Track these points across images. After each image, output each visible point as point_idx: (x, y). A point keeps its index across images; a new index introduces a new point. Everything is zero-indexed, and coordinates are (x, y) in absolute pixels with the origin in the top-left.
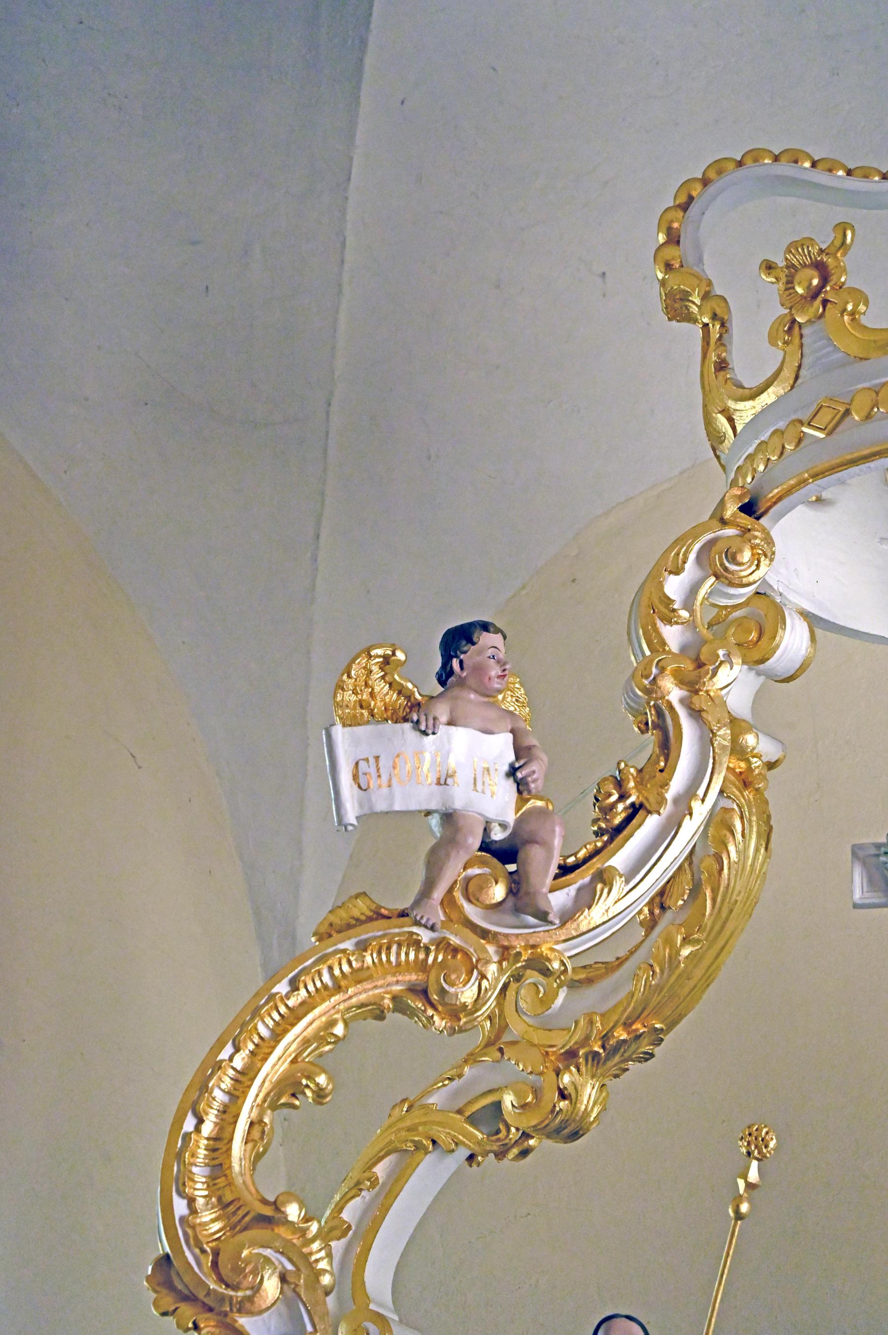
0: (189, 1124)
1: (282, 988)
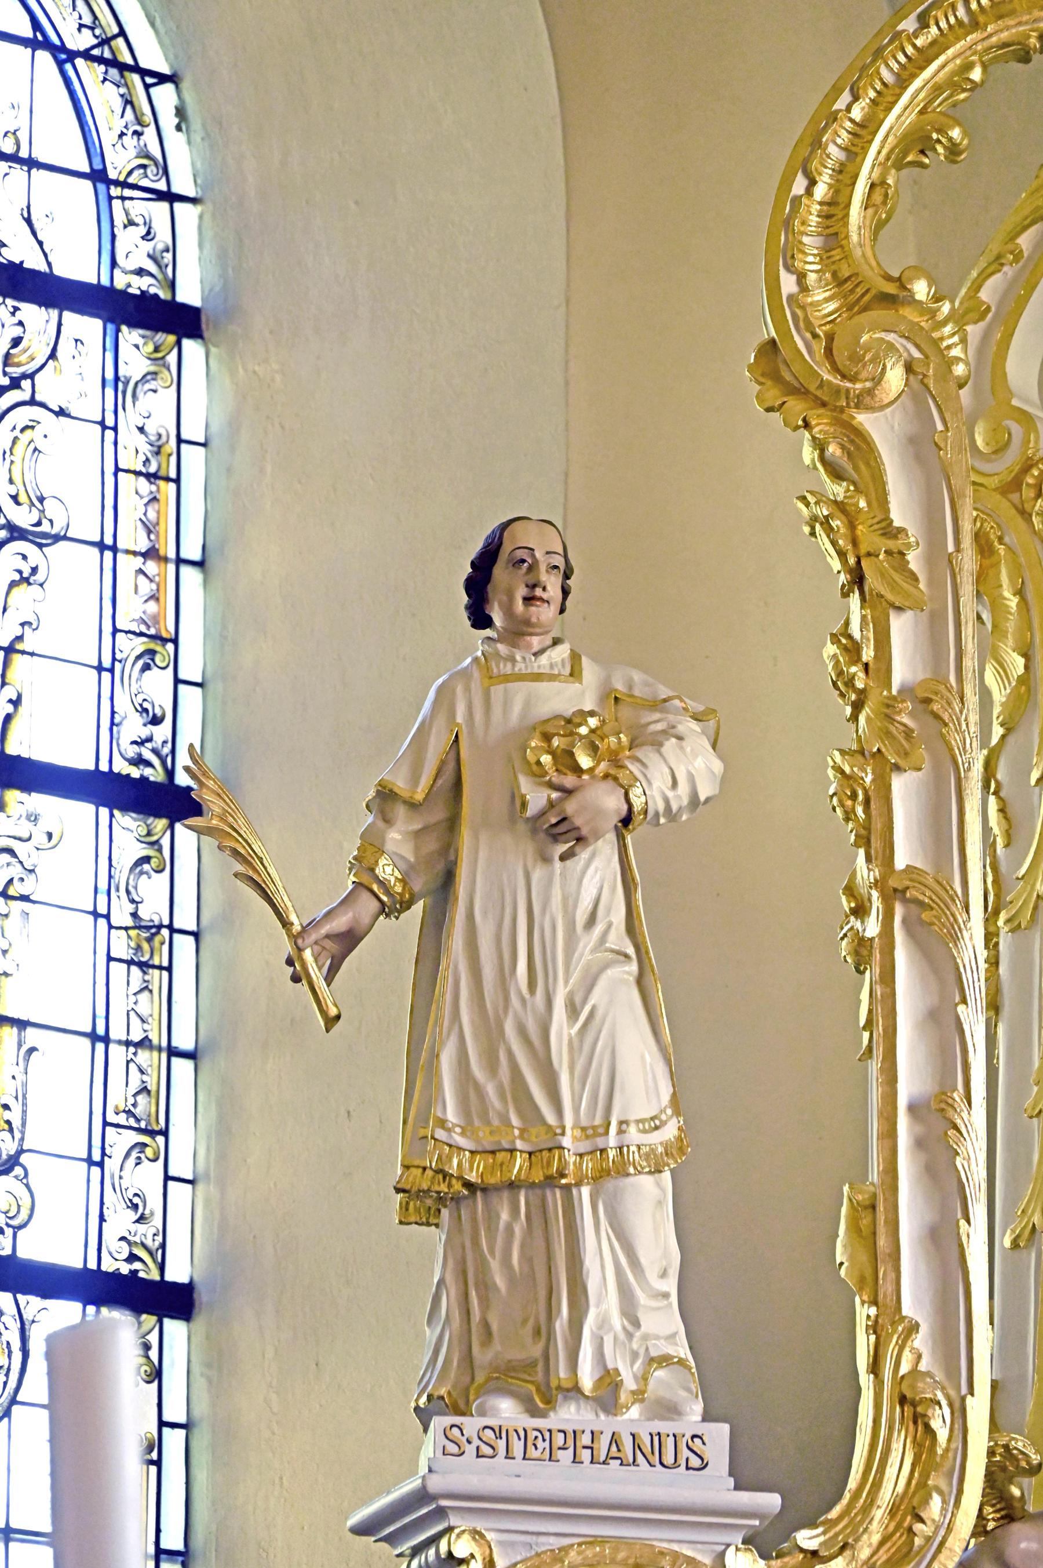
0: (799, 186)
1: (909, 24)
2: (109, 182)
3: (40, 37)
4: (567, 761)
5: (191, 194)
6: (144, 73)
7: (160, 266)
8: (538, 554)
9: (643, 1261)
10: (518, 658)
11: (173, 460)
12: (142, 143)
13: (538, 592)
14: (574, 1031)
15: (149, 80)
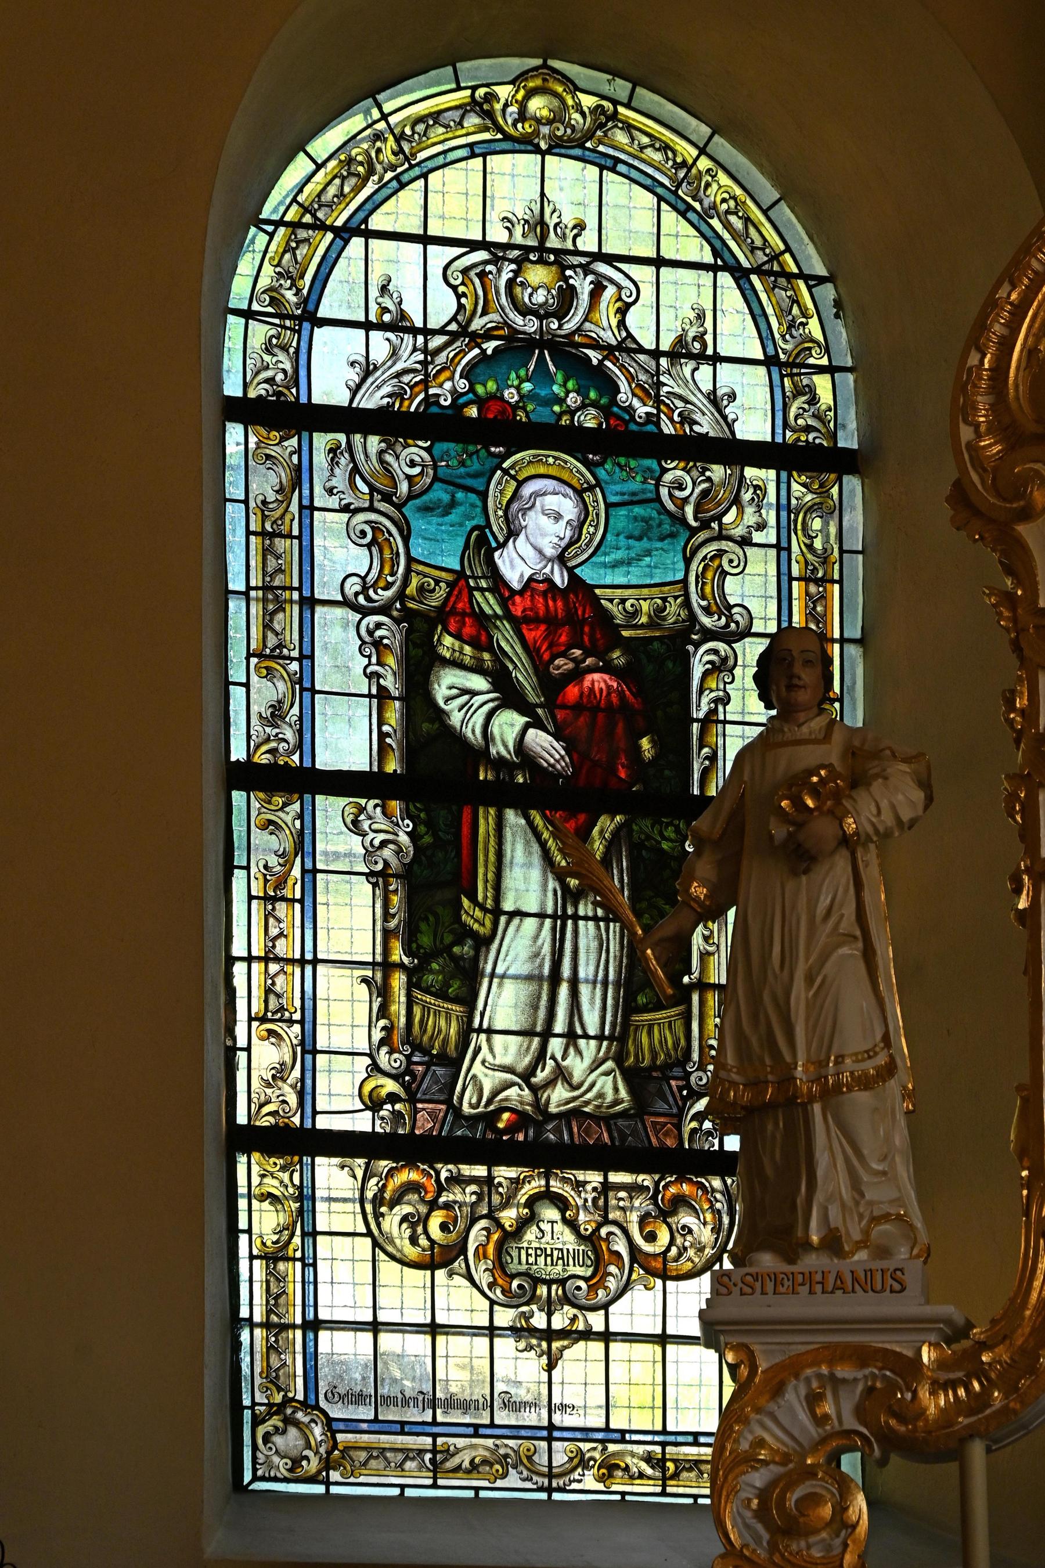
2: (780, 365)
3: (719, 262)
5: (849, 364)
6: (806, 278)
7: (823, 423)
8: (795, 654)
9: (865, 1152)
10: (786, 729)
11: (837, 567)
12: (807, 331)
13: (796, 681)
14: (811, 993)
15: (812, 283)
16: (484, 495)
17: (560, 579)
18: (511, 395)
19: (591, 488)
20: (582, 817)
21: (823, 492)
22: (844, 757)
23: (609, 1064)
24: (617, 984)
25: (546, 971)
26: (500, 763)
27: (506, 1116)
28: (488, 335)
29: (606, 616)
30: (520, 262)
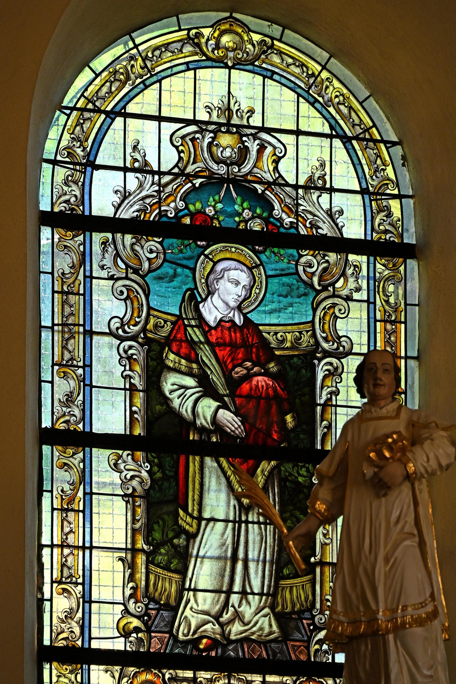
2: (370, 194)
3: (334, 133)
4: (380, 455)
5: (411, 193)
6: (385, 142)
7: (395, 228)
8: (379, 365)
9: (420, 664)
10: (373, 410)
11: (403, 313)
12: (385, 174)
13: (379, 382)
14: (388, 568)
15: (388, 145)
16: (193, 270)
17: (238, 320)
18: (210, 211)
19: (257, 266)
20: (251, 462)
21: (395, 269)
22: (407, 427)
23: (267, 610)
24: (272, 562)
25: (229, 554)
26: (202, 430)
27: (205, 641)
28: (196, 175)
29: (265, 343)
30: (215, 132)
